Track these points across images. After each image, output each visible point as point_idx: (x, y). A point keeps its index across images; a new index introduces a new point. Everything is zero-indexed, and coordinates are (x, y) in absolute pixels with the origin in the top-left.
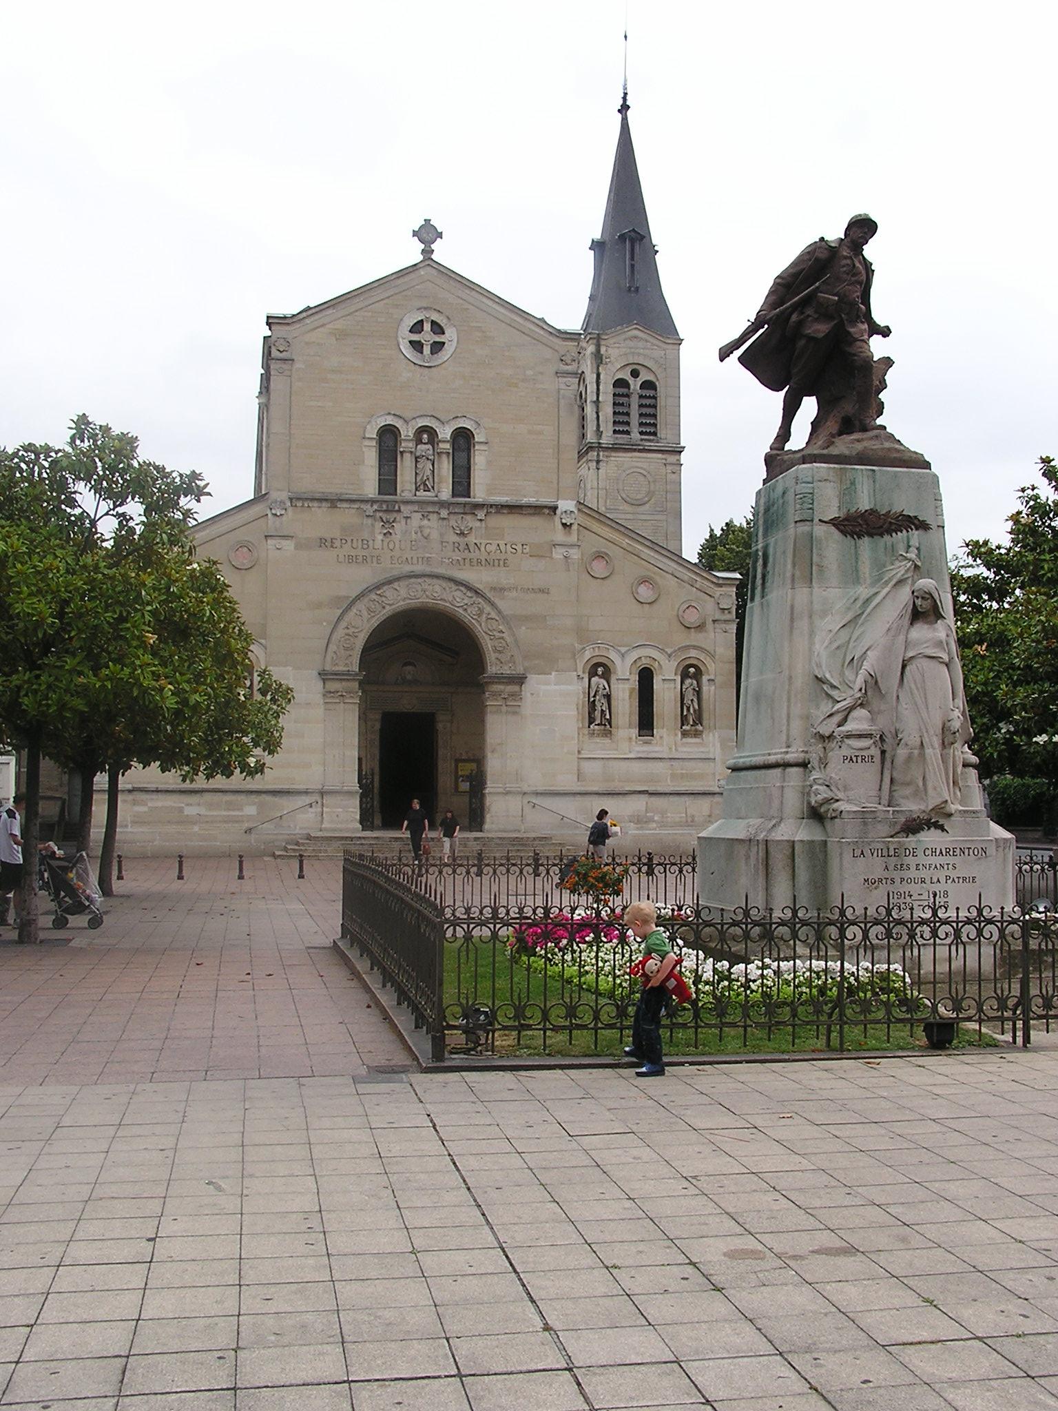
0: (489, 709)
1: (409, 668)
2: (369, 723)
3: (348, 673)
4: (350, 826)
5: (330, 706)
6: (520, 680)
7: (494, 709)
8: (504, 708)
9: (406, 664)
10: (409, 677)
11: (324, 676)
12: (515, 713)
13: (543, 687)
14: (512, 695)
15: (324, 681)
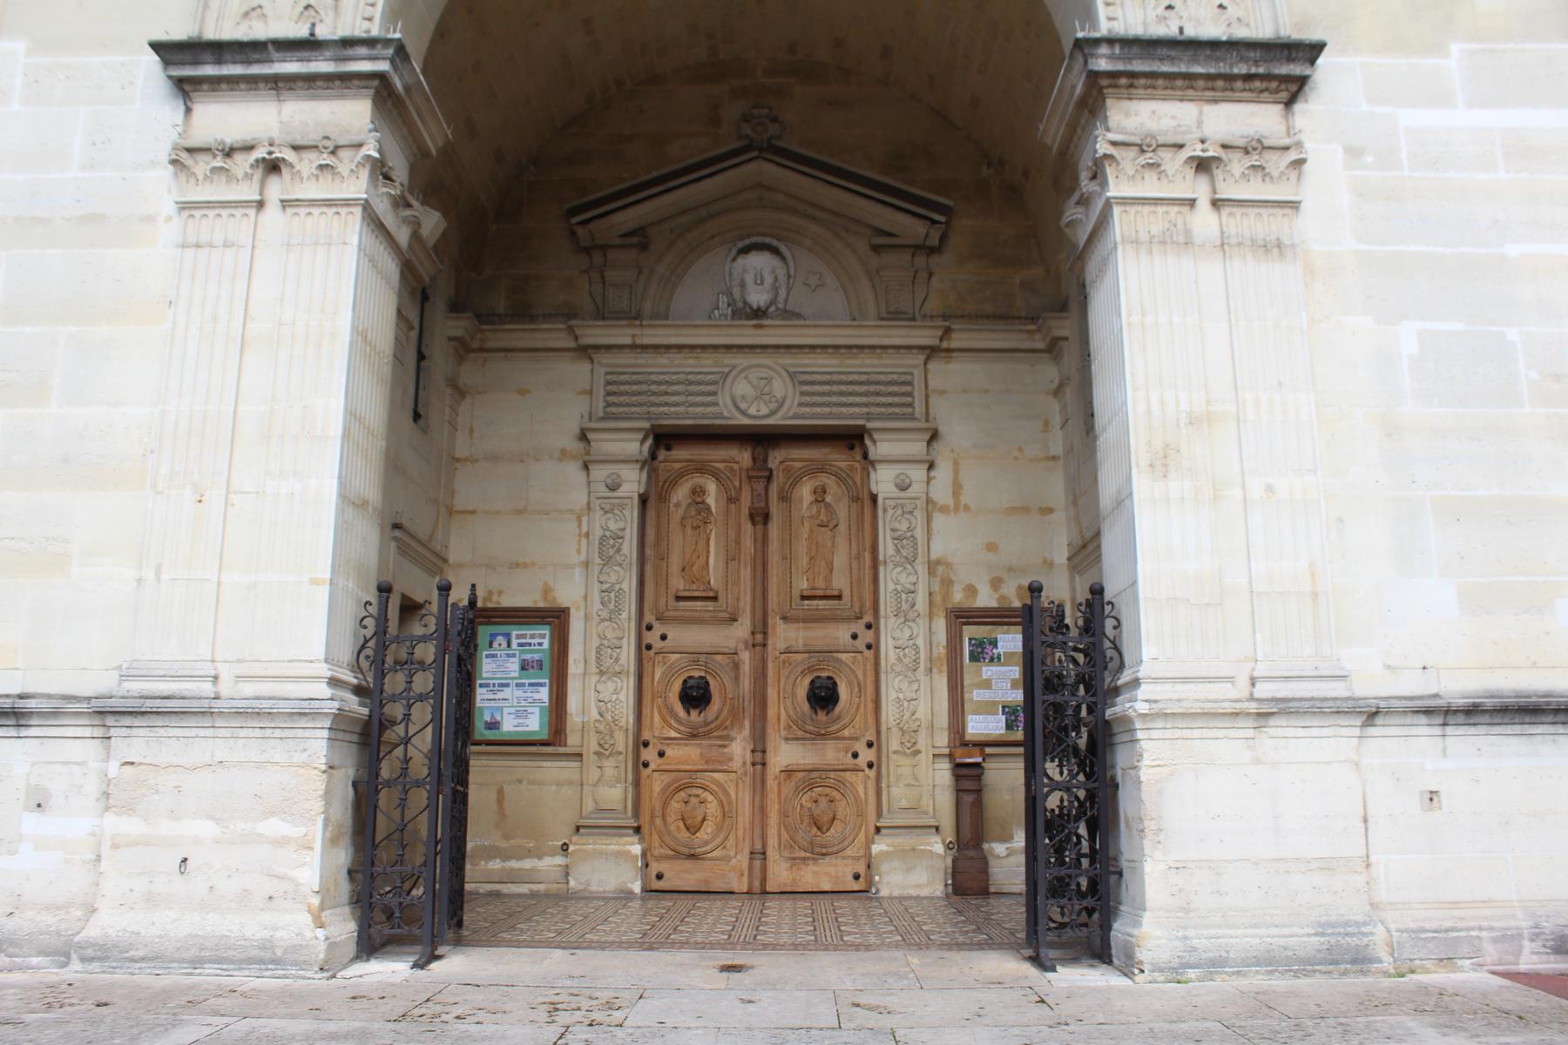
0: (1122, 223)
1: (759, 262)
2: (600, 473)
3: (308, 45)
4: (248, 927)
5: (211, 227)
6: (1279, 67)
7: (1151, 222)
8: (1204, 221)
9: (745, 250)
10: (758, 298)
11: (193, 64)
12: (1274, 248)
13: (1411, 117)
14: (1254, 147)
15: (186, 88)
